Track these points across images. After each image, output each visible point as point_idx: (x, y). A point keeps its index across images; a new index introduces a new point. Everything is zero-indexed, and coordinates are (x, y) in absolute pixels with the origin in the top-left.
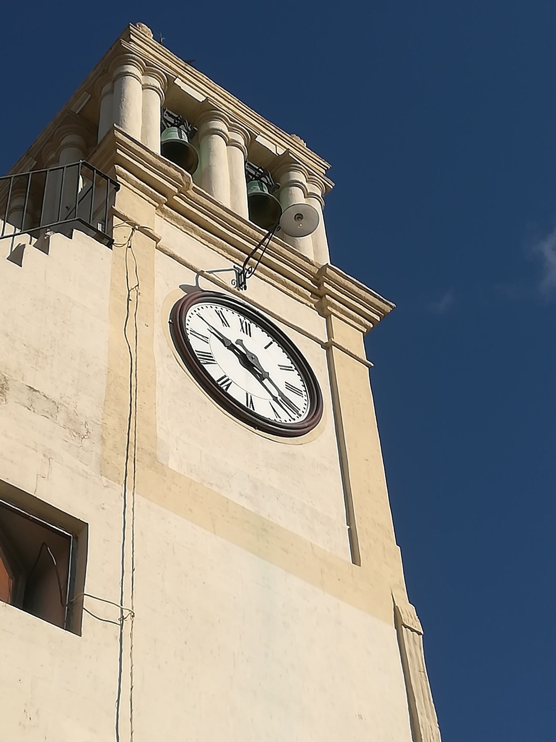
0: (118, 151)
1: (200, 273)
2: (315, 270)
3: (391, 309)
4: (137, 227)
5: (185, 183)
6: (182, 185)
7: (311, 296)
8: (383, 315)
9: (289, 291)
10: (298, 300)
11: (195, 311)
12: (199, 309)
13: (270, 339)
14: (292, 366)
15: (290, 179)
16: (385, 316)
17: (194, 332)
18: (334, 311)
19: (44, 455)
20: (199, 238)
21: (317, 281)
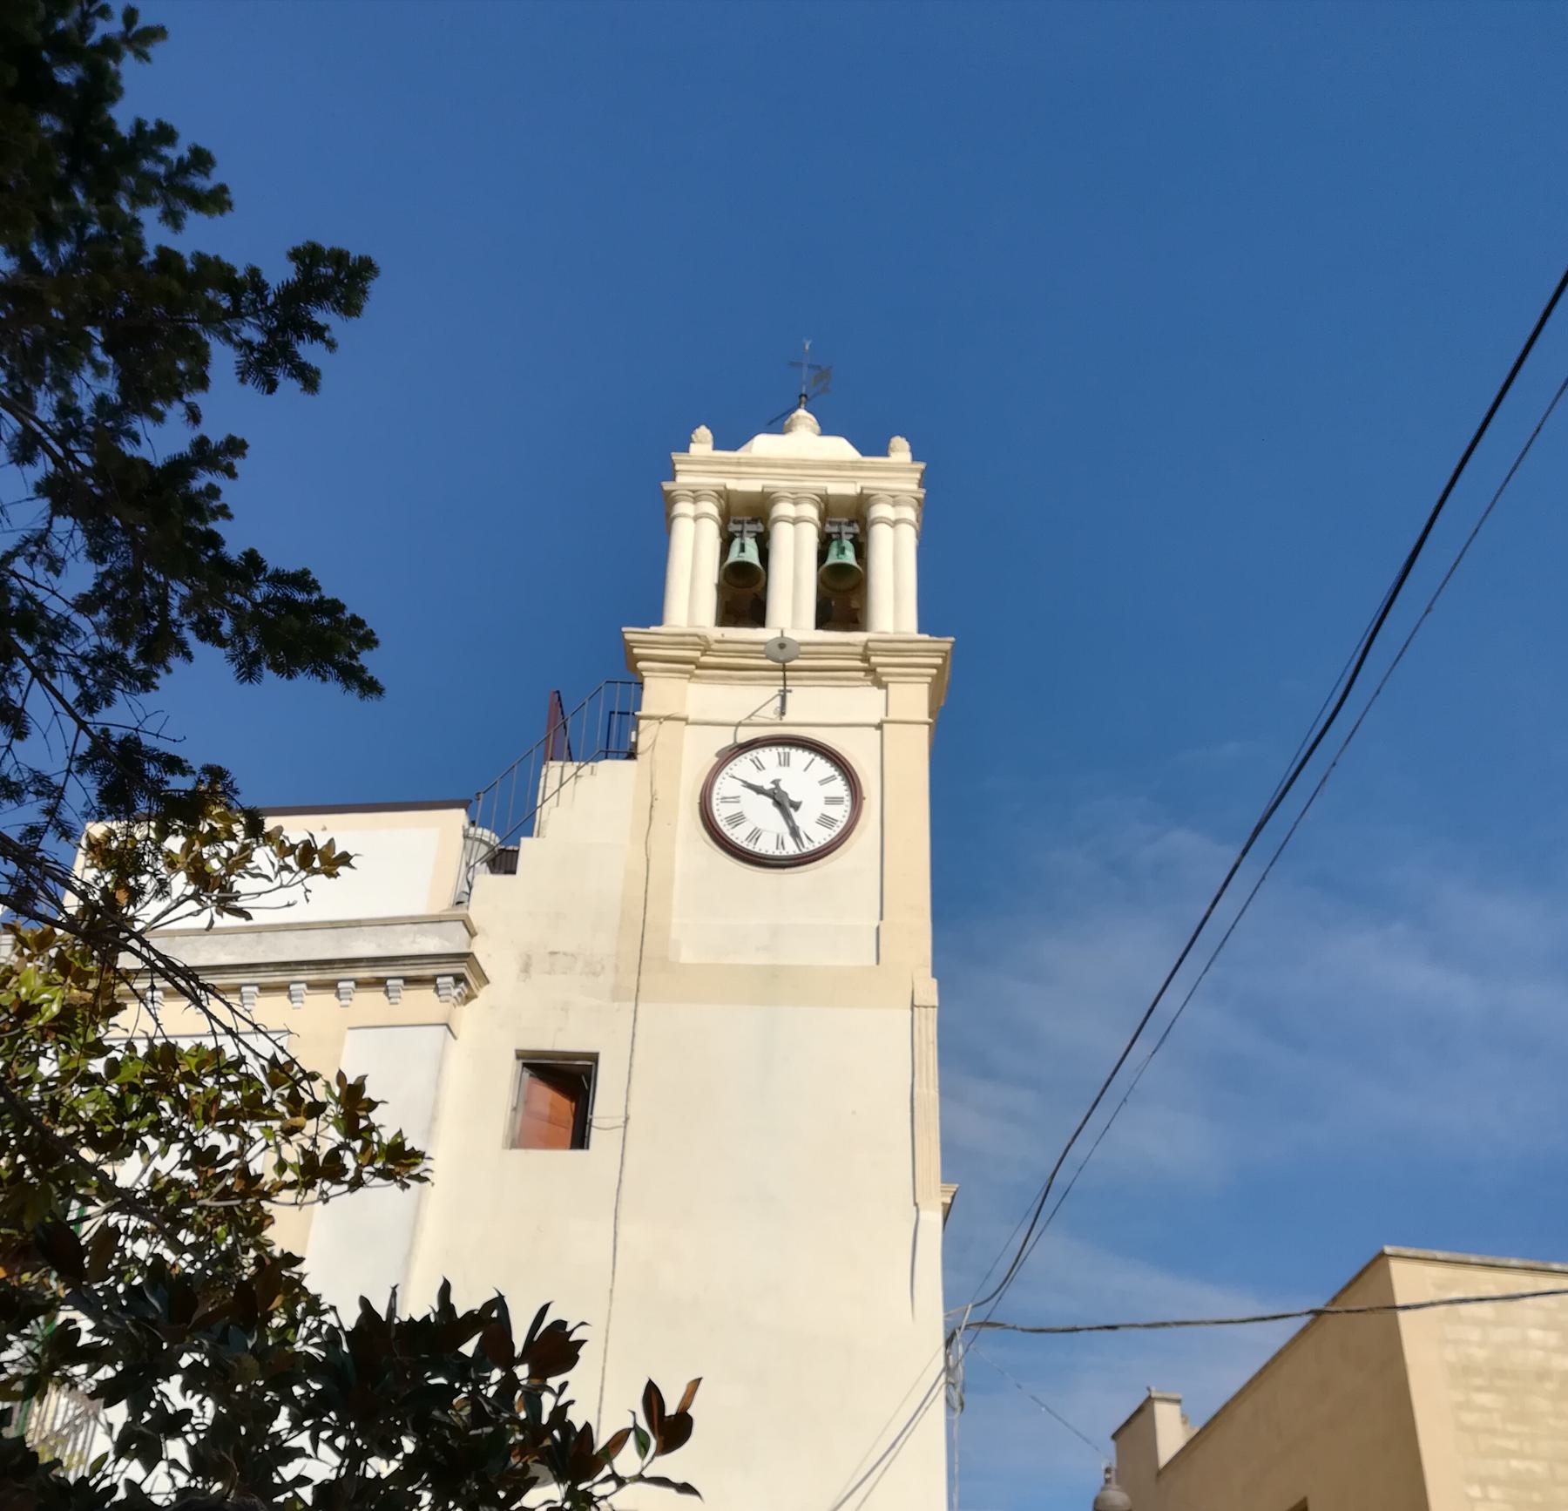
1: (739, 724)
2: (860, 650)
6: (700, 645)
7: (865, 676)
11: (727, 774)
12: (731, 769)
13: (812, 756)
14: (837, 773)
16: (945, 655)
17: (725, 798)
19: (562, 1009)
20: (739, 682)
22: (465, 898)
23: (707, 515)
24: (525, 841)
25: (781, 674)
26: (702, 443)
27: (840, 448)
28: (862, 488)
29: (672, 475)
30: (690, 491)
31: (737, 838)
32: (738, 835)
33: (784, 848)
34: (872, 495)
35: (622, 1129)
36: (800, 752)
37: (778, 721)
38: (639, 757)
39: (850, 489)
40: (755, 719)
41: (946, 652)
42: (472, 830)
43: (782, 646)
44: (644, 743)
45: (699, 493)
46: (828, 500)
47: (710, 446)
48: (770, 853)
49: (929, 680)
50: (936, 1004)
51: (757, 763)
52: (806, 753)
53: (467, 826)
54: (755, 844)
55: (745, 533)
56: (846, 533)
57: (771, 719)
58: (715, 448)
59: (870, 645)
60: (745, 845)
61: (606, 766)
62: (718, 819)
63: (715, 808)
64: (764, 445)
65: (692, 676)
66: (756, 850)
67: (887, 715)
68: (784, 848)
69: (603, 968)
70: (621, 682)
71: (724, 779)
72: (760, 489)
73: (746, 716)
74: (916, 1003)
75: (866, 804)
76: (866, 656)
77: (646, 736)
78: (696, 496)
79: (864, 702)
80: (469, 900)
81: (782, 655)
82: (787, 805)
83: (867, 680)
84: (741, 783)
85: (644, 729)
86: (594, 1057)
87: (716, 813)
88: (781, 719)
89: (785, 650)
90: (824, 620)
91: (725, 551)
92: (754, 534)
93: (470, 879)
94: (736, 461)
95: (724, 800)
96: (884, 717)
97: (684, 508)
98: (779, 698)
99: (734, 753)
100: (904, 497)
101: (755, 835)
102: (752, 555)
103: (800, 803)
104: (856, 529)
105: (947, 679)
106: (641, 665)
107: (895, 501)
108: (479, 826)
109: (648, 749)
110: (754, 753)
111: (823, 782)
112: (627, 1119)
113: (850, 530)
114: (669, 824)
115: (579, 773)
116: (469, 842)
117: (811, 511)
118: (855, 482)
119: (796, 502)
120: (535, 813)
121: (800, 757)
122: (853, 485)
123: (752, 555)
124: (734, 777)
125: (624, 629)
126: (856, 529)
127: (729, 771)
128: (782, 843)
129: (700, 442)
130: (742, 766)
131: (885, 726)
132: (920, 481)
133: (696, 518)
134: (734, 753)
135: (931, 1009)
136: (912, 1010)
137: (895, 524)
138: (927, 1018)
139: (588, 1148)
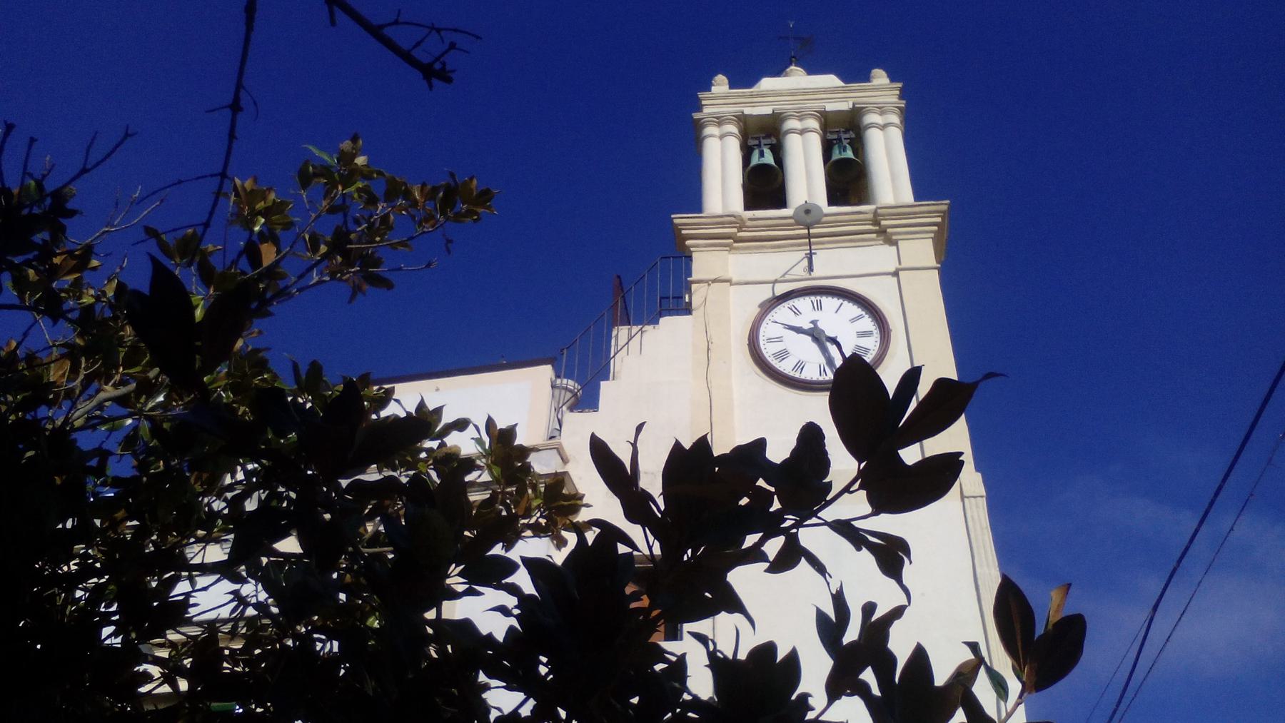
1: (775, 282)
2: (870, 216)
5: (739, 221)
7: (877, 236)
10: (868, 246)
13: (841, 301)
14: (864, 313)
22: (556, 433)
23: (731, 134)
24: (602, 383)
25: (807, 240)
26: (721, 85)
27: (831, 80)
28: (854, 104)
29: (699, 108)
30: (714, 117)
32: (786, 367)
33: (826, 375)
34: (864, 108)
36: (830, 298)
37: (808, 276)
38: (694, 312)
39: (845, 106)
40: (787, 277)
41: (944, 212)
42: (559, 381)
43: (807, 212)
44: (696, 301)
45: (723, 118)
46: (826, 116)
47: (728, 87)
48: (815, 379)
49: (932, 235)
50: (982, 491)
51: (794, 309)
52: (835, 299)
53: (554, 378)
55: (762, 146)
56: (845, 139)
58: (731, 87)
59: (879, 211)
60: (792, 374)
61: (669, 323)
62: (767, 356)
63: (762, 347)
64: (767, 83)
65: (731, 248)
66: (803, 377)
67: (900, 263)
68: (826, 375)
72: (771, 112)
73: (782, 274)
75: (893, 335)
76: (876, 220)
77: (698, 295)
78: (720, 121)
79: (881, 256)
80: (560, 435)
81: (808, 219)
82: (824, 339)
83: (879, 240)
84: (782, 326)
85: (695, 291)
87: (764, 352)
88: (810, 274)
89: (810, 215)
90: (833, 199)
91: (746, 159)
92: (769, 146)
93: (560, 417)
94: (749, 94)
95: (769, 340)
97: (709, 130)
99: (773, 304)
101: (800, 366)
102: (769, 159)
104: (852, 135)
106: (689, 242)
107: (882, 111)
108: (565, 377)
109: (701, 304)
110: (791, 303)
111: (854, 320)
113: (847, 136)
114: (725, 362)
115: (643, 329)
116: (557, 392)
117: (813, 124)
119: (801, 118)
120: (609, 362)
121: (830, 303)
122: (846, 103)
123: (769, 159)
124: (776, 322)
125: (673, 216)
126: (852, 135)
129: (719, 85)
130: (782, 313)
131: (900, 273)
133: (722, 137)
134: (773, 304)
137: (883, 127)
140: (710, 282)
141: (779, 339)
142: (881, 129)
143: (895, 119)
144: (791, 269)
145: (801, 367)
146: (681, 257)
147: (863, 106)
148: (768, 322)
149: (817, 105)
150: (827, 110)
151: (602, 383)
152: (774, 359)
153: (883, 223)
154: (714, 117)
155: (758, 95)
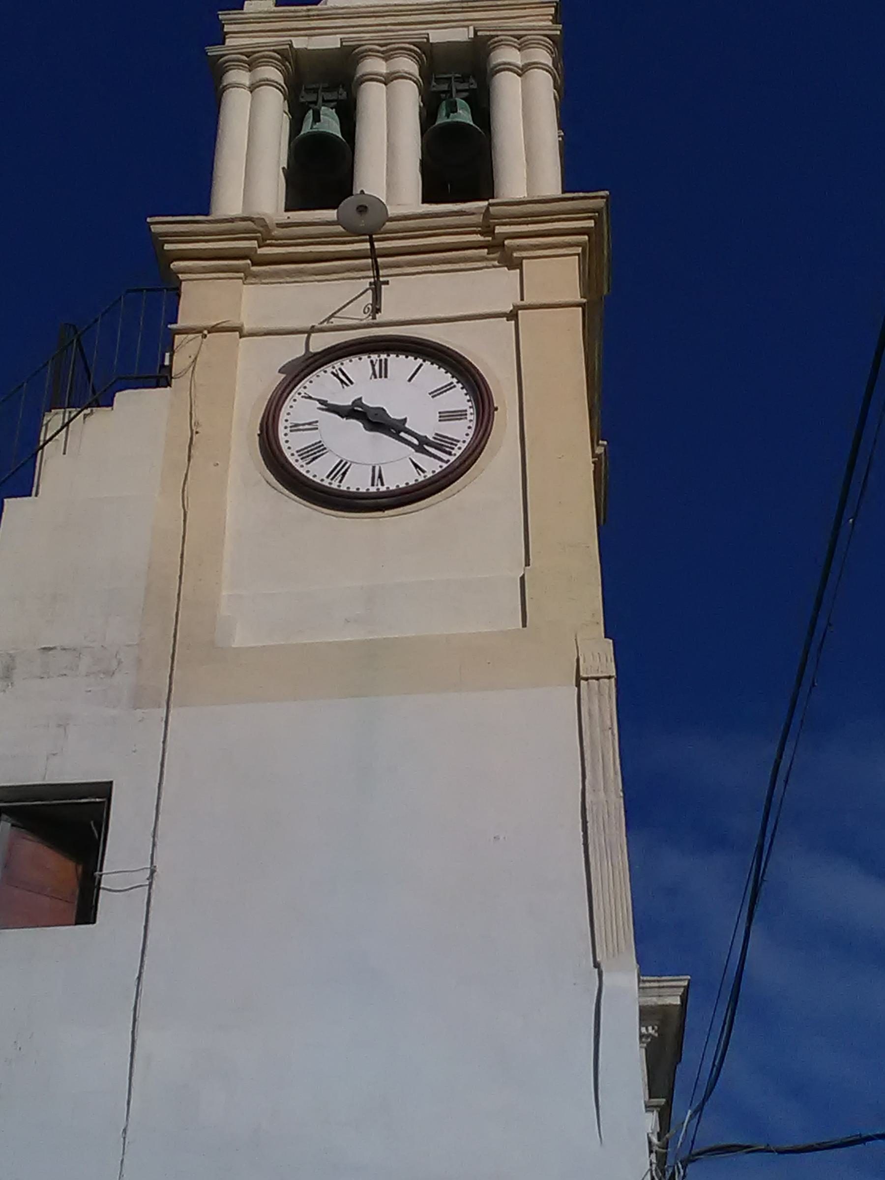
0: (167, 247)
1: (313, 330)
2: (478, 219)
3: (605, 200)
4: (206, 332)
5: (261, 229)
6: (259, 232)
7: (488, 253)
8: (597, 214)
9: (457, 266)
11: (299, 394)
12: (305, 387)
13: (420, 361)
14: (455, 380)
15: (489, 65)
17: (296, 425)
18: (524, 254)
21: (489, 229)
28: (475, 32)
30: (242, 54)
31: (315, 476)
33: (382, 484)
35: (147, 888)
37: (370, 320)
39: (462, 35)
40: (335, 322)
44: (180, 361)
45: (257, 55)
49: (579, 250)
50: (614, 674)
52: (411, 358)
54: (340, 481)
56: (458, 91)
57: (361, 320)
60: (326, 483)
62: (287, 454)
65: (248, 276)
66: (344, 488)
67: (522, 299)
68: (382, 484)
69: (120, 662)
70: (148, 290)
71: (295, 400)
74: (583, 674)
78: (252, 61)
81: (362, 222)
83: (493, 259)
86: (105, 790)
87: (284, 446)
88: (374, 318)
90: (427, 198)
95: (295, 428)
96: (519, 302)
97: (238, 76)
98: (370, 292)
100: (531, 35)
102: (330, 123)
103: (405, 420)
105: (605, 252)
106: (175, 265)
109: (186, 371)
110: (337, 365)
111: (435, 394)
112: (153, 872)
113: (465, 86)
117: (408, 65)
118: (468, 26)
119: (387, 57)
123: (330, 123)
124: (310, 398)
125: (149, 220)
127: (302, 391)
128: (380, 477)
132: (555, 16)
133: (252, 88)
135: (606, 680)
136: (578, 685)
137: (522, 71)
138: (600, 693)
139: (94, 922)
140: (206, 332)
141: (312, 426)
142: (520, 75)
143: (544, 57)
144: (339, 310)
145: (343, 470)
146: (162, 290)
147: (488, 33)
148: (297, 397)
149: (417, 33)
150: (431, 41)
151: (5, 500)
152: (299, 458)
153: (498, 229)
154: (242, 54)
155: (320, 17)
